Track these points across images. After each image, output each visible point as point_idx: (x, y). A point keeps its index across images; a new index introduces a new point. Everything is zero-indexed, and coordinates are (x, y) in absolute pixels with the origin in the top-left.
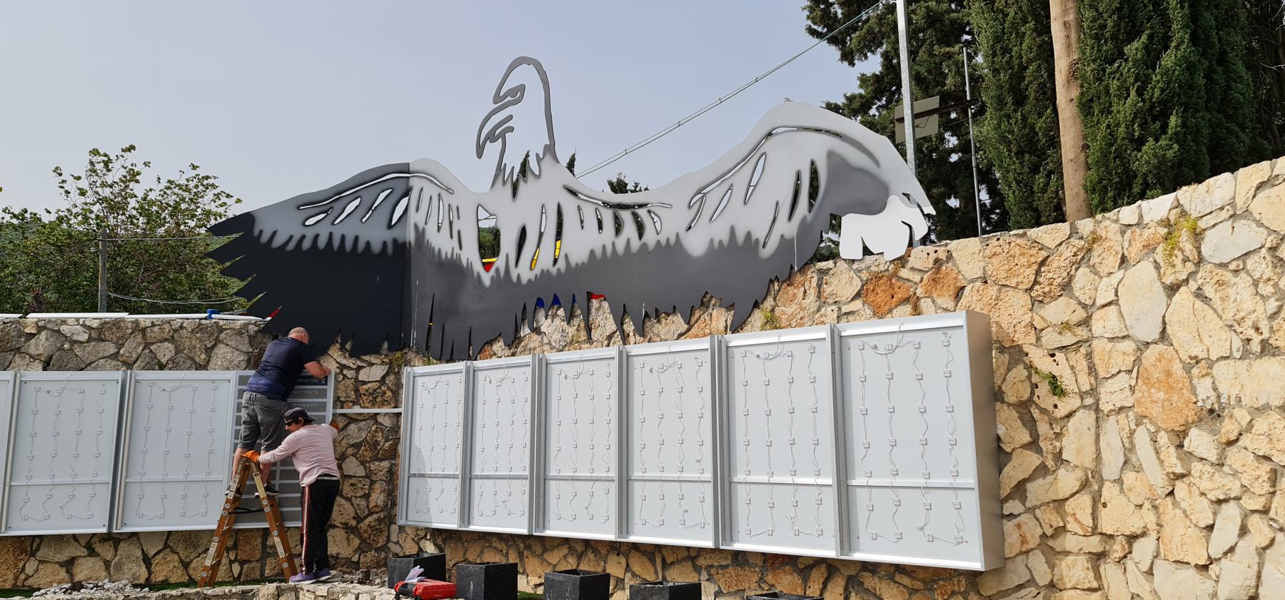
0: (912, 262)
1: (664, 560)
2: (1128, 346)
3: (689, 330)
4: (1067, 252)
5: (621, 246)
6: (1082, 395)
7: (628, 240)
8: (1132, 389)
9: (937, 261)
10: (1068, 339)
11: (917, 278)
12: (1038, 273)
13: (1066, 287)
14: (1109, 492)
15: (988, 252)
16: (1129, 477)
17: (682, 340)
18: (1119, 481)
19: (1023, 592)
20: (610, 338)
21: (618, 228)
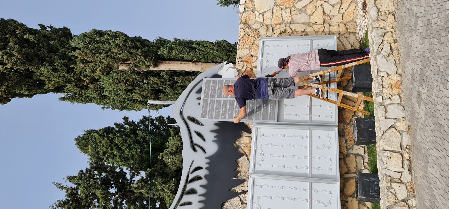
0: (240, 68)
1: (347, 173)
2: (275, 9)
3: (247, 155)
4: (247, 30)
5: (201, 191)
6: (286, 26)
7: (201, 186)
8: (286, 8)
9: (241, 62)
10: (271, 29)
11: (245, 67)
12: (251, 36)
13: (256, 30)
14: (312, 21)
15: (242, 48)
16: (309, 12)
17: (250, 160)
18: (310, 16)
19: (342, 40)
20: (243, 203)
21: (193, 192)
